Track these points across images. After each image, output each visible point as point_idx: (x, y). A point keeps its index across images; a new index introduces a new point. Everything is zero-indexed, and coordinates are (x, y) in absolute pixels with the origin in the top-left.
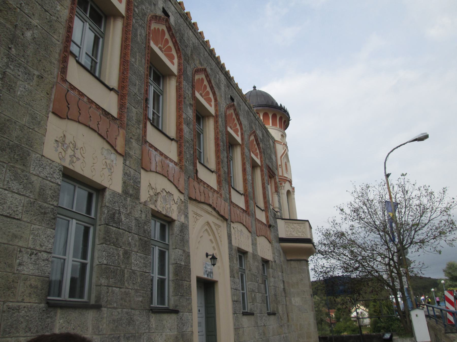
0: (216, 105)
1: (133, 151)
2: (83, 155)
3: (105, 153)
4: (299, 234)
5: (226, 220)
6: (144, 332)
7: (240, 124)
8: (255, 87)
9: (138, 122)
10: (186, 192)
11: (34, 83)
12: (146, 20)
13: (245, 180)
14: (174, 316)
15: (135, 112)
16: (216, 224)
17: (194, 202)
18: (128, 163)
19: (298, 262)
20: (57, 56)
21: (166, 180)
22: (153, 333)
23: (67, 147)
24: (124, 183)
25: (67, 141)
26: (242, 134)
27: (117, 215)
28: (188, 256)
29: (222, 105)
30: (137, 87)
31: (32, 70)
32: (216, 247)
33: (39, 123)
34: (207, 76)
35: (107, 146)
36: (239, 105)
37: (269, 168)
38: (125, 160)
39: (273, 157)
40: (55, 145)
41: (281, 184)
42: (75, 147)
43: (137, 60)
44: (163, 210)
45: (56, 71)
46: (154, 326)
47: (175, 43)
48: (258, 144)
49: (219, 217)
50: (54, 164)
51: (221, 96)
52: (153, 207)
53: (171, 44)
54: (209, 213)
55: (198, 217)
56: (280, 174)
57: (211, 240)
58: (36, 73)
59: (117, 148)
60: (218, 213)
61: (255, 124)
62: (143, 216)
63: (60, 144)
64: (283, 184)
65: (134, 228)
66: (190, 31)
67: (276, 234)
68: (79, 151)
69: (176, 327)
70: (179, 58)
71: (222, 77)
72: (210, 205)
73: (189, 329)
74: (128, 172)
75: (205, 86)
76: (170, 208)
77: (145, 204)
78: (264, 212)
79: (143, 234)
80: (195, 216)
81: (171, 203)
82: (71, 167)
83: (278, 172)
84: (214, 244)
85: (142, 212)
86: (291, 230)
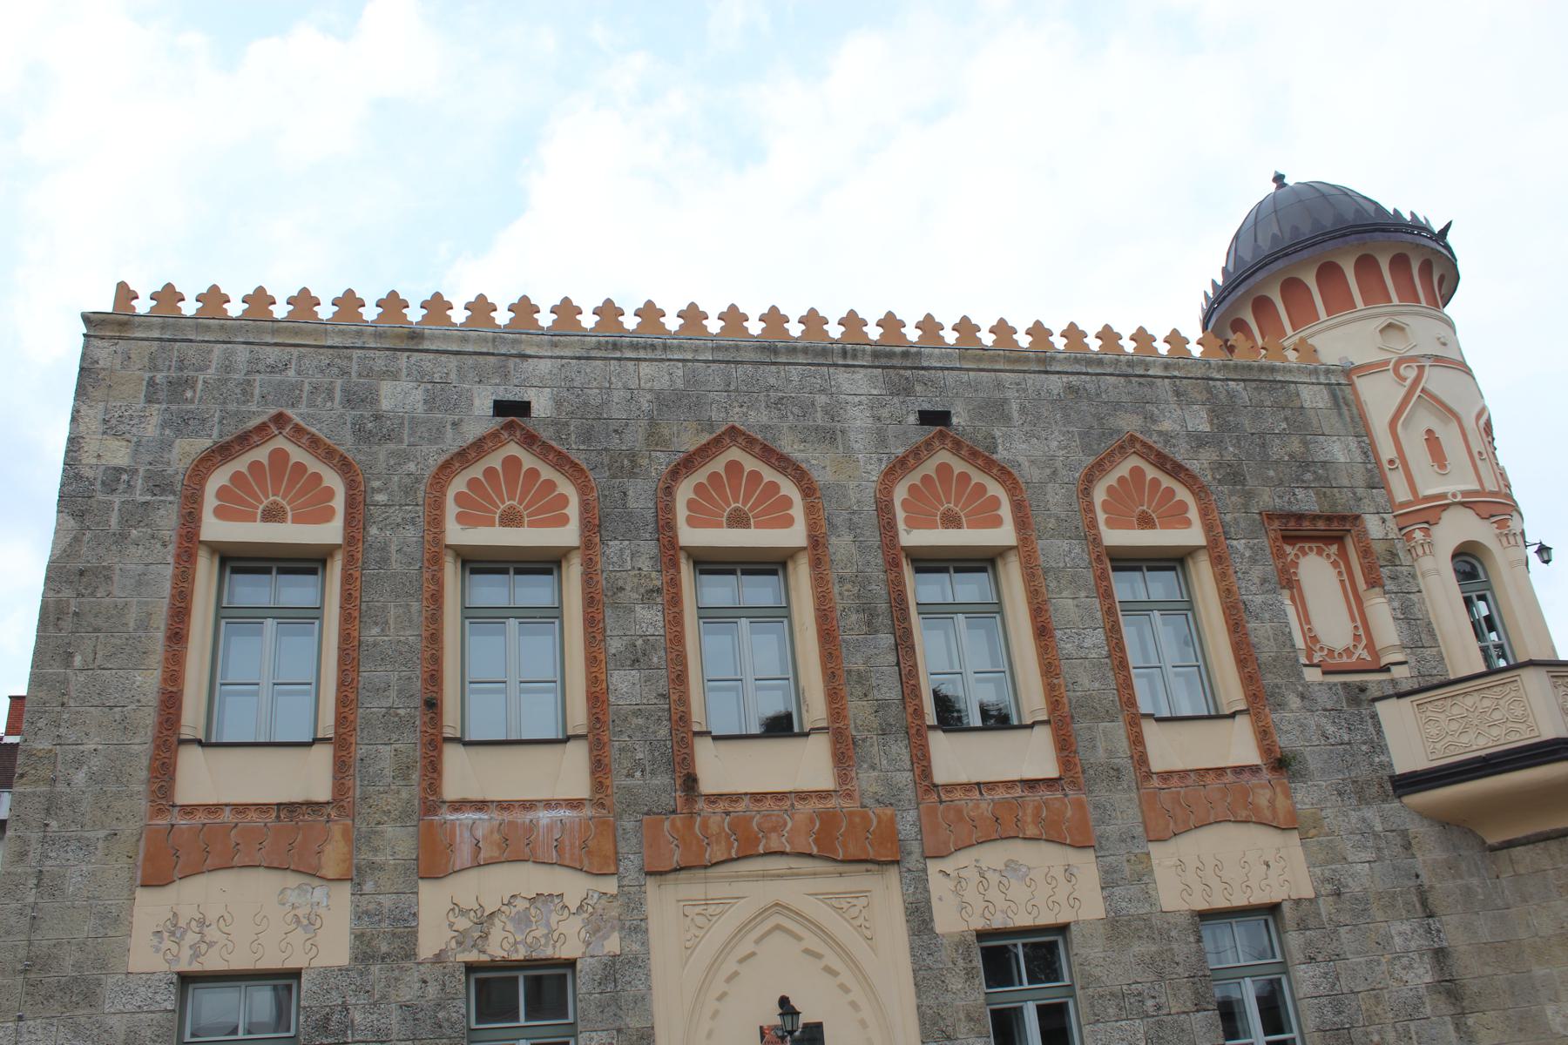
0: (810, 510)
1: (388, 851)
2: (226, 929)
3: (292, 897)
4: (1495, 731)
5: (897, 862)
7: (1005, 475)
8: (1279, 179)
9: (403, 772)
10: (631, 864)
11: (100, 853)
12: (421, 494)
13: (1049, 669)
15: (384, 755)
17: (683, 875)
18: (368, 887)
20: (144, 774)
21: (529, 866)
23: (185, 931)
24: (358, 936)
25: (182, 923)
26: (1018, 507)
27: (336, 1017)
29: (852, 484)
30: (393, 693)
31: (92, 834)
32: (837, 964)
33: (115, 921)
34: (750, 443)
35: (293, 880)
36: (996, 410)
37: (1288, 516)
38: (358, 886)
39: (1340, 451)
40: (155, 941)
41: (1409, 537)
42: (202, 923)
43: (391, 621)
45: (143, 805)
47: (562, 462)
48: (1176, 470)
50: (155, 977)
51: (849, 453)
52: (473, 956)
53: (547, 473)
54: (780, 876)
55: (711, 909)
56: (1401, 493)
57: (807, 951)
58: (102, 834)
59: (323, 872)
60: (835, 860)
61: (1141, 405)
62: (432, 991)
63: (166, 935)
64: (1418, 535)
65: (395, 1028)
66: (644, 365)
67: (1363, 771)
68: (214, 926)
70: (584, 489)
71: (857, 385)
72: (783, 853)
74: (372, 907)
75: (755, 476)
76: (546, 936)
77: (439, 958)
78: (1243, 722)
80: (698, 909)
81: (554, 918)
82: (196, 967)
83: (1390, 492)
84: (832, 960)
85: (425, 982)
86: (1454, 726)
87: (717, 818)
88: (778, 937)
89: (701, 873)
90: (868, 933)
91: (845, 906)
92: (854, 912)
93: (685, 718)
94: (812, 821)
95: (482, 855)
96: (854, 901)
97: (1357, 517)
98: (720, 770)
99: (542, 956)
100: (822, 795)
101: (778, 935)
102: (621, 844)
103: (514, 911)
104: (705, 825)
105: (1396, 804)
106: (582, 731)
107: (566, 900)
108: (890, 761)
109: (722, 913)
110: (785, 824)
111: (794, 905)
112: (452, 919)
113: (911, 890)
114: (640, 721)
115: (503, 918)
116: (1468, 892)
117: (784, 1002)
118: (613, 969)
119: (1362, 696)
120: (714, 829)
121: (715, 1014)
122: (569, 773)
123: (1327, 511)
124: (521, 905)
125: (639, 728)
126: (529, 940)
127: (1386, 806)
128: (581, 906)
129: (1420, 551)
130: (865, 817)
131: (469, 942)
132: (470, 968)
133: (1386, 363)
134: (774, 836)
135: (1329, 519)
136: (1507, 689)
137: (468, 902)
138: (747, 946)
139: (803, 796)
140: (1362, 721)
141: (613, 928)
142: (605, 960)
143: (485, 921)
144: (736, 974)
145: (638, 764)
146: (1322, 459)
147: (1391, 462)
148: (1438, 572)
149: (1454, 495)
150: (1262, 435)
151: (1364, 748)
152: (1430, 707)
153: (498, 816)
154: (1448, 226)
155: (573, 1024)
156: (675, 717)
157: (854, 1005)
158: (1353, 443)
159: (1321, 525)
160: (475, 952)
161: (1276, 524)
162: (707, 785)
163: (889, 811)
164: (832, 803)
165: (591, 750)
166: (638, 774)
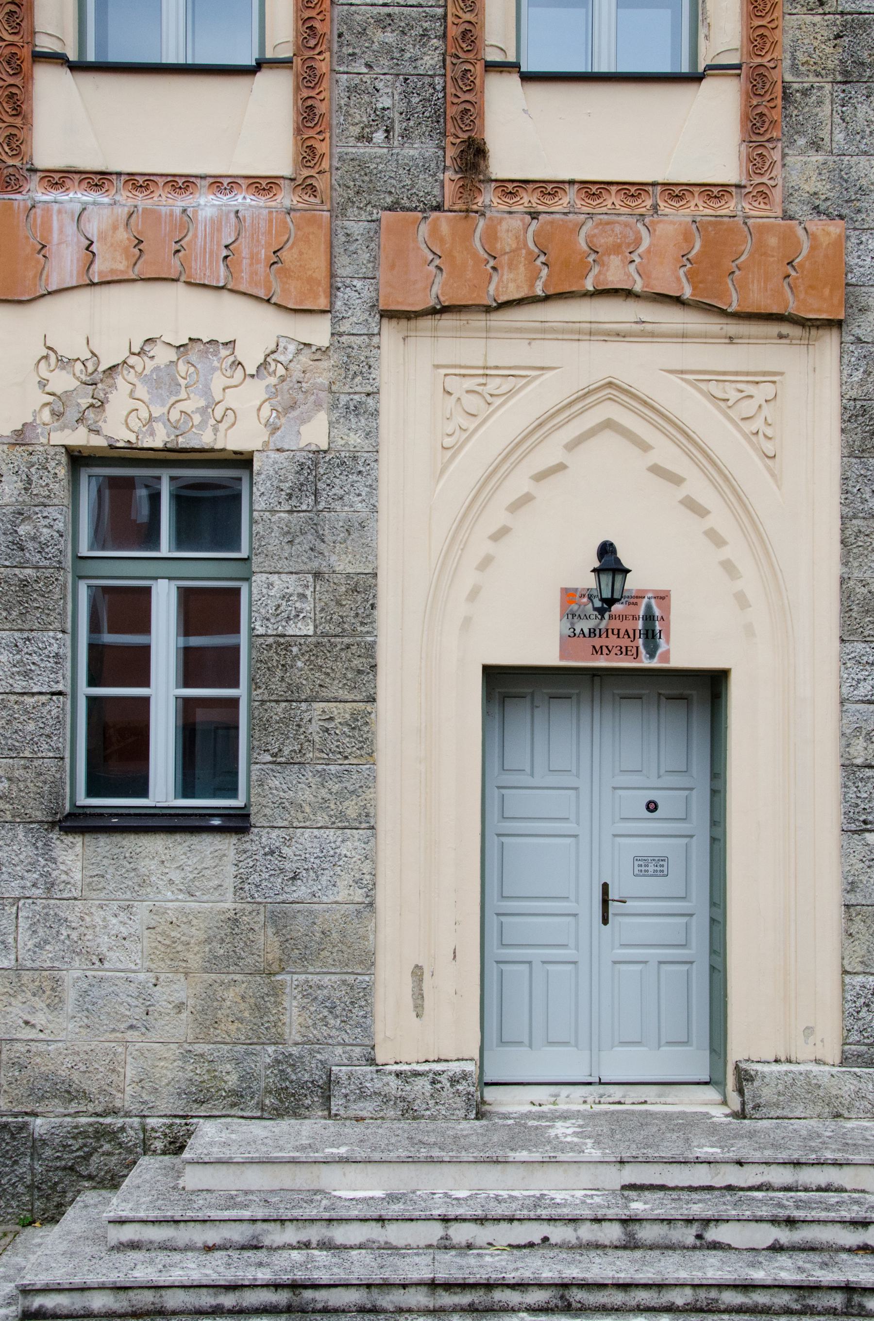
6: (17, 894)
14: (227, 845)
16: (697, 377)
17: (447, 321)
21: (179, 290)
22: (75, 899)
28: (363, 589)
32: (706, 496)
44: (152, 434)
46: (78, 876)
49: (734, 328)
52: (79, 438)
55: (493, 385)
57: (656, 470)
69: (229, 883)
72: (628, 294)
73: (344, 892)
76: (203, 411)
79: (9, 557)
80: (470, 384)
81: (218, 382)
87: (516, 222)
88: (609, 440)
89: (478, 321)
90: (769, 447)
91: (733, 396)
92: (748, 408)
93: (470, 36)
94: (687, 238)
95: (96, 267)
96: (750, 389)
98: (524, 134)
99: (195, 444)
100: (714, 192)
101: (608, 438)
102: (342, 260)
103: (150, 365)
104: (491, 235)
106: (286, 53)
107: (241, 354)
108: (851, 135)
109: (511, 393)
110: (638, 241)
111: (643, 388)
112: (45, 374)
113: (858, 375)
114: (390, 37)
115: (132, 377)
117: (606, 550)
118: (313, 474)
120: (507, 241)
121: (486, 562)
122: (254, 130)
124: (163, 355)
125: (387, 49)
126: (174, 415)
128: (264, 364)
130: (788, 238)
131: (72, 414)
132: (78, 459)
134: (615, 261)
137: (71, 346)
138: (550, 453)
139: (676, 192)
141: (318, 405)
142: (300, 457)
143: (101, 378)
144: (527, 498)
145: (380, 116)
153: (126, 199)
155: (247, 559)
156: (454, 31)
157: (729, 567)
160: (82, 430)
162: (502, 163)
163: (835, 228)
164: (732, 205)
165: (297, 89)
166: (379, 136)
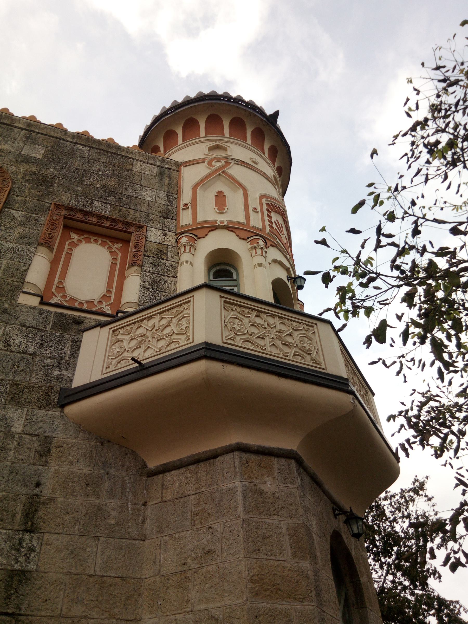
19: (202, 467)
86: (133, 343)
97: (141, 227)
105: (56, 413)
116: (98, 513)
119: (75, 327)
123: (117, 216)
127: (41, 412)
129: (182, 250)
133: (205, 159)
135: (114, 221)
136: (182, 309)
140: (60, 341)
146: (131, 194)
147: (186, 205)
148: (192, 264)
149: (222, 222)
150: (87, 172)
151: (48, 361)
152: (121, 331)
154: (277, 114)
158: (162, 195)
159: (107, 224)
161: (64, 212)
